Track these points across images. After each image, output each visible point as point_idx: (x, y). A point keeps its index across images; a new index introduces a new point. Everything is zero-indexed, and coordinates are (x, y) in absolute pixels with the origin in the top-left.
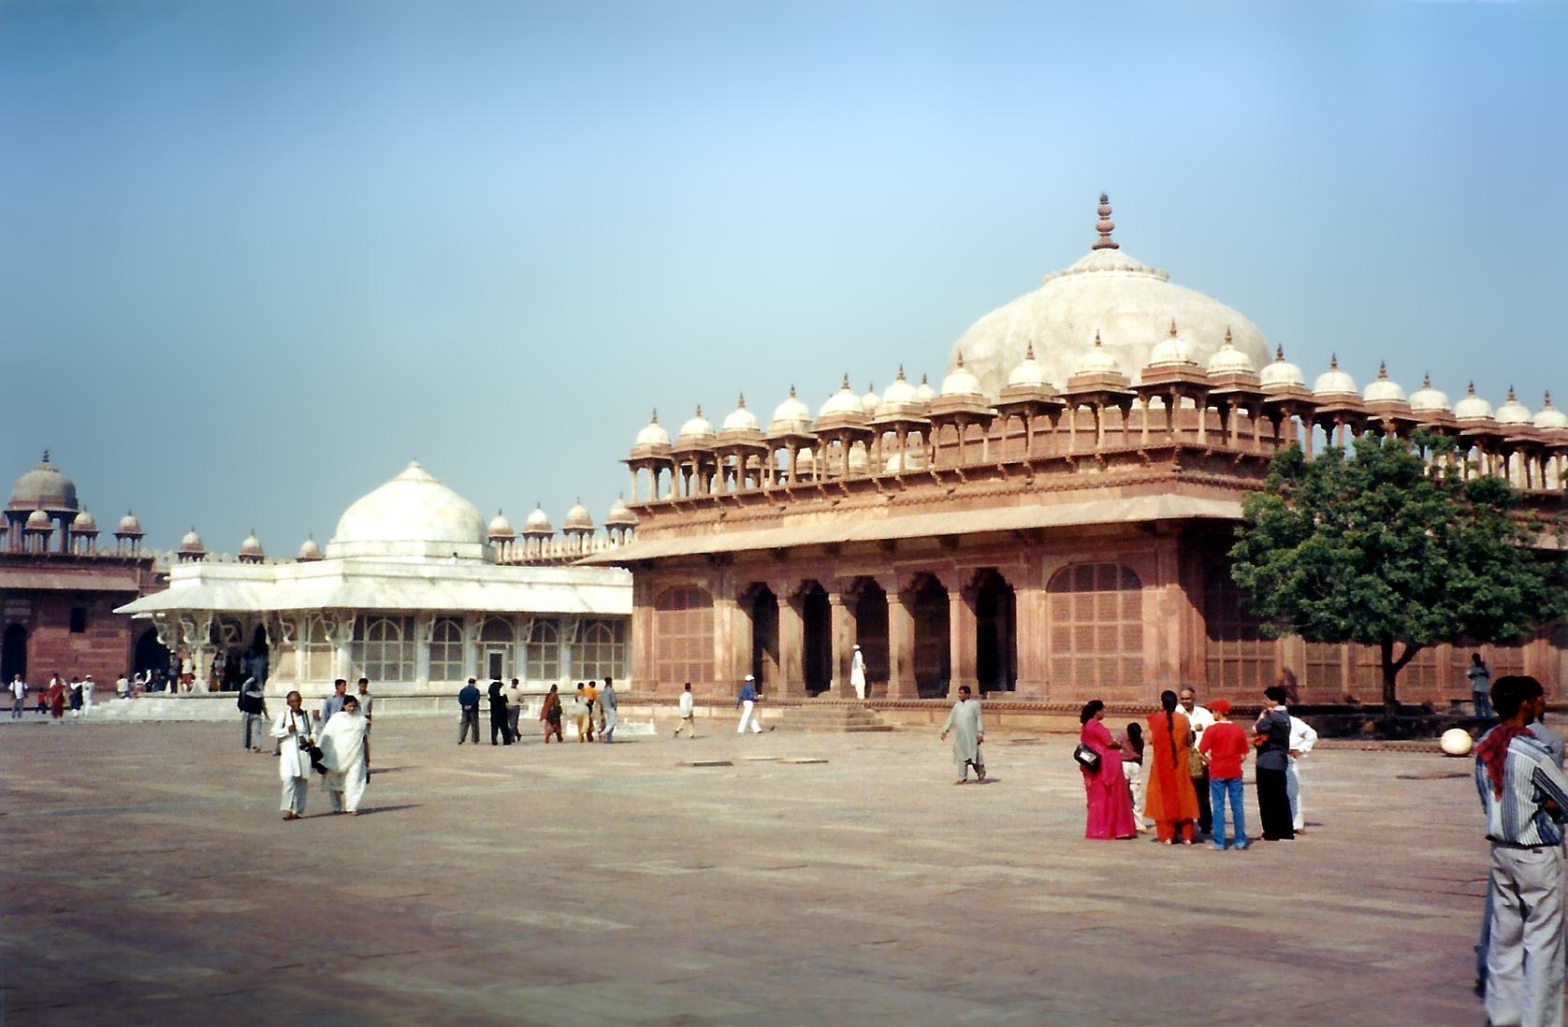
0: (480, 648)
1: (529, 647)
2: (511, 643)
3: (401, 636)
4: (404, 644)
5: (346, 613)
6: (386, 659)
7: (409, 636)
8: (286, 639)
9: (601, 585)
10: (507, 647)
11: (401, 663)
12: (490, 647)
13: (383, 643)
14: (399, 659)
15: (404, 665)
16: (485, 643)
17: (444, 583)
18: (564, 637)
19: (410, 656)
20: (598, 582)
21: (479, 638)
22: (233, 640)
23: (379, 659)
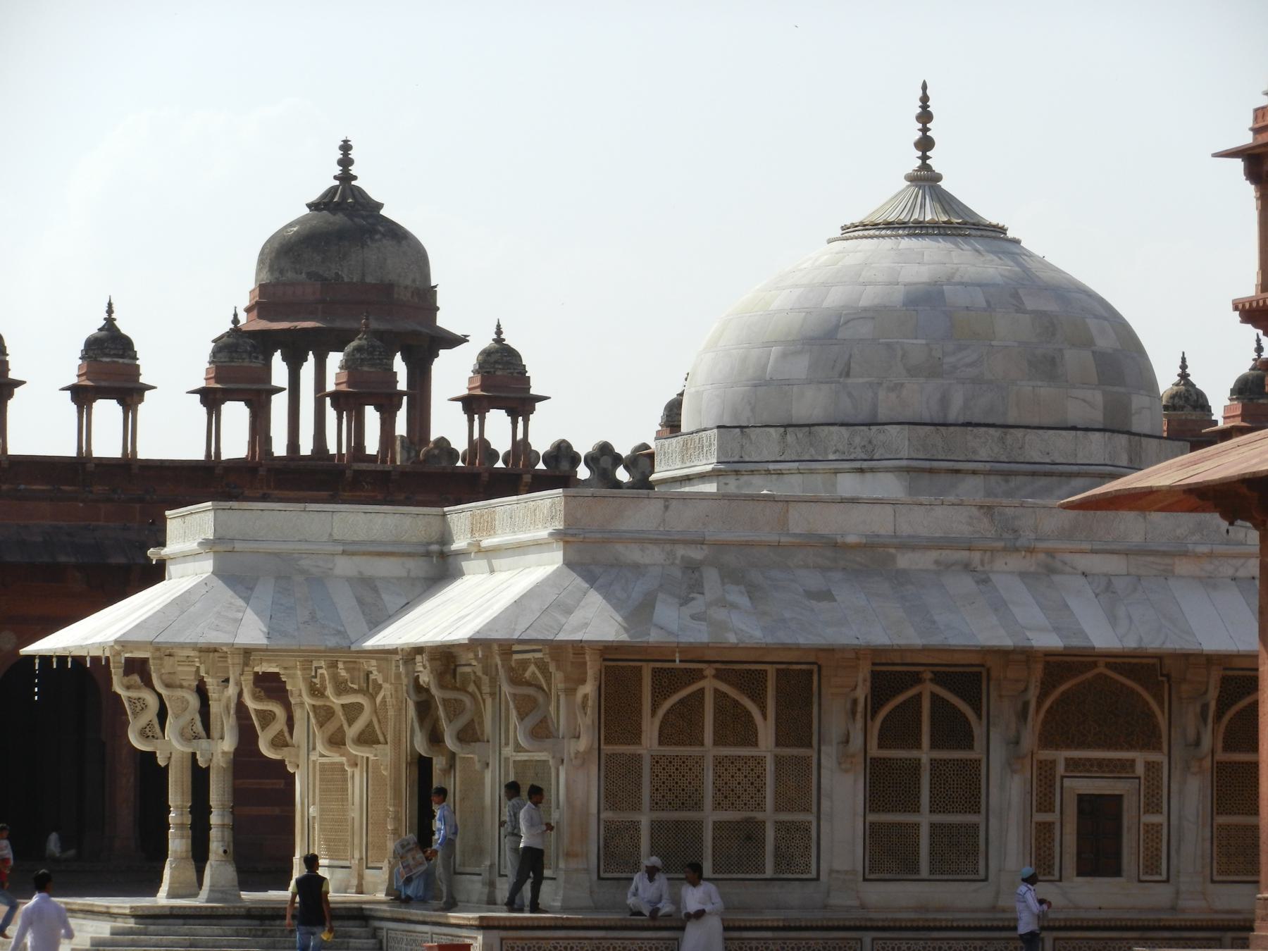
2: (1153, 757)
3: (766, 731)
4: (779, 760)
6: (718, 806)
10: (1140, 770)
11: (769, 815)
14: (760, 806)
16: (1062, 755)
23: (698, 806)
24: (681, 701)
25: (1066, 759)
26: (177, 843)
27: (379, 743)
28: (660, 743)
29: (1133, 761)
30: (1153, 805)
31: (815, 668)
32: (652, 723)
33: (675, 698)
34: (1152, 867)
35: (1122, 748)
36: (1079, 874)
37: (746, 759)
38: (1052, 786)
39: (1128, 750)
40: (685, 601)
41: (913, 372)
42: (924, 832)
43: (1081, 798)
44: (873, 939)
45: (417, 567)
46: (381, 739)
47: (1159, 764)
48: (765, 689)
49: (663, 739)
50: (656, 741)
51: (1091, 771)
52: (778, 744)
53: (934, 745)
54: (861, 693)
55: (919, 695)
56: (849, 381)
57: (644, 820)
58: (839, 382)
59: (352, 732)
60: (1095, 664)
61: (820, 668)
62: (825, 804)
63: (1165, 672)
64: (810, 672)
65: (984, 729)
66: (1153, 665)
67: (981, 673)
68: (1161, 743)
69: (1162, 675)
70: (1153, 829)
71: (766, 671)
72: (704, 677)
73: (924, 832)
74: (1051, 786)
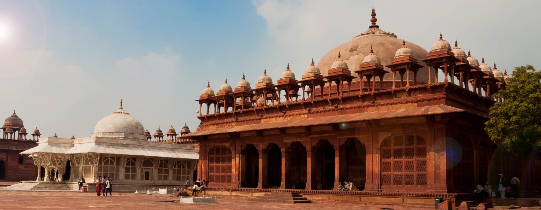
2: (152, 168)
3: (115, 164)
5: (95, 155)
7: (118, 164)
8: (76, 164)
10: (151, 169)
12: (145, 168)
13: (109, 166)
19: (118, 170)
20: (182, 148)
21: (142, 165)
22: (59, 164)
24: (107, 160)
26: (39, 175)
29: (150, 168)
30: (152, 173)
33: (106, 160)
34: (152, 179)
43: (146, 172)
45: (70, 145)
52: (116, 165)
54: (126, 160)
57: (102, 173)
62: (121, 172)
70: (152, 175)
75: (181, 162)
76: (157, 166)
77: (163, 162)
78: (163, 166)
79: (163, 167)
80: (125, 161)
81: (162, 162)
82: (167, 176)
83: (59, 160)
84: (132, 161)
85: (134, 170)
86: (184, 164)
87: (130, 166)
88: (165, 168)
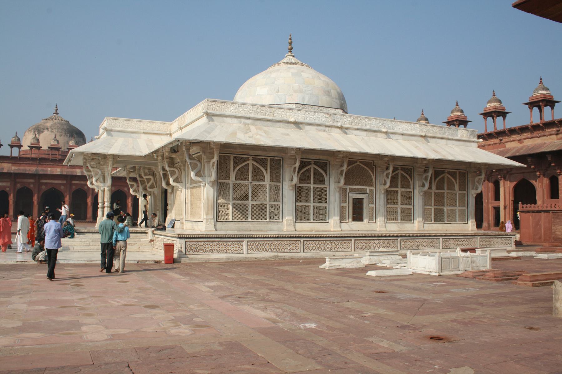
0: (343, 191)
1: (387, 192)
3: (267, 177)
6: (253, 199)
7: (276, 177)
9: (447, 139)
11: (268, 203)
12: (353, 191)
14: (265, 200)
15: (271, 206)
17: (307, 128)
18: (417, 184)
19: (276, 194)
20: (445, 136)
21: (342, 181)
23: (247, 199)
24: (242, 167)
25: (349, 188)
27: (155, 188)
28: (236, 180)
29: (366, 189)
31: (281, 159)
32: (233, 173)
35: (363, 186)
36: (353, 221)
37: (261, 185)
38: (346, 196)
39: (365, 186)
40: (246, 133)
41: (295, 91)
42: (312, 208)
44: (304, 241)
46: (156, 187)
47: (373, 190)
48: (267, 165)
49: (237, 178)
50: (234, 179)
51: (355, 192)
53: (314, 183)
54: (297, 165)
55: (310, 168)
56: (278, 94)
58: (275, 94)
59: (148, 185)
60: (357, 162)
61: (283, 159)
63: (375, 164)
64: (280, 160)
65: (328, 179)
66: (371, 162)
67: (327, 162)
68: (373, 184)
69: (374, 165)
71: (267, 159)
72: (249, 160)
73: (312, 208)
74: (345, 196)
75: (443, 172)
76: (385, 184)
77: (400, 172)
78: (399, 184)
79: (399, 186)
80: (295, 168)
81: (398, 174)
82: (410, 209)
83: (150, 177)
84: (314, 168)
85: (322, 196)
86: (451, 178)
87: (310, 183)
88: (404, 190)
